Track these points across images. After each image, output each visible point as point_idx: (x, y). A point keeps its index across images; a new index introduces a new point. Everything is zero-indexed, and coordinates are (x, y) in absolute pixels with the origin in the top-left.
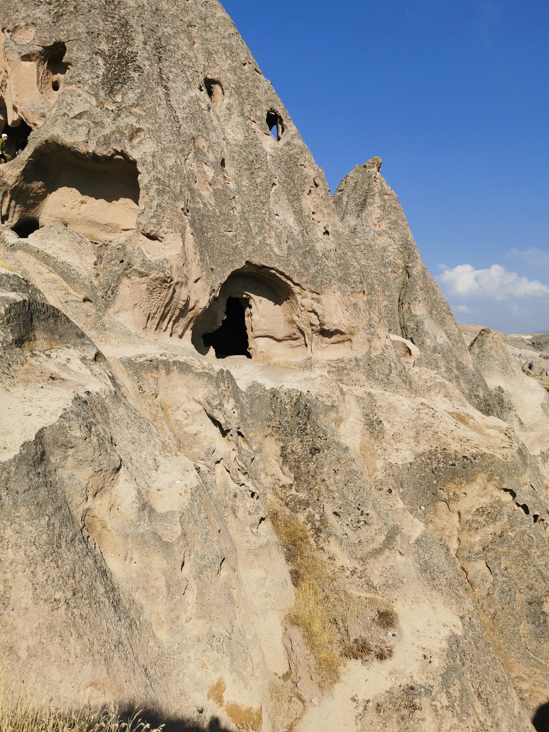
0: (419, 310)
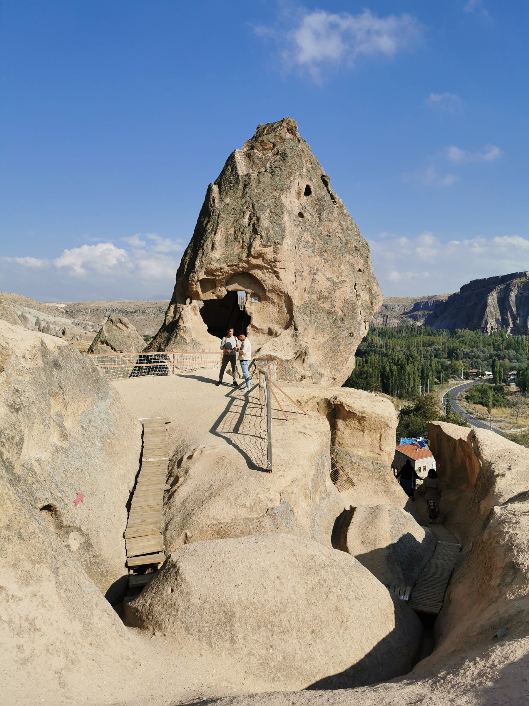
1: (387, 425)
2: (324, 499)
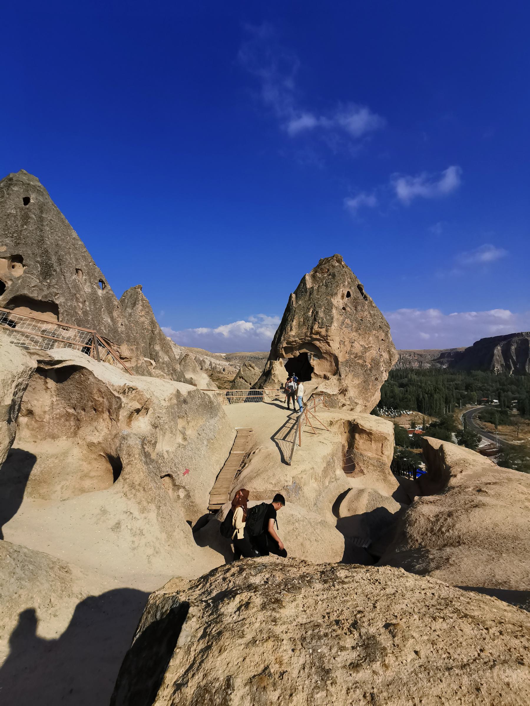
0: (157, 348)
1: (386, 438)
2: (333, 482)
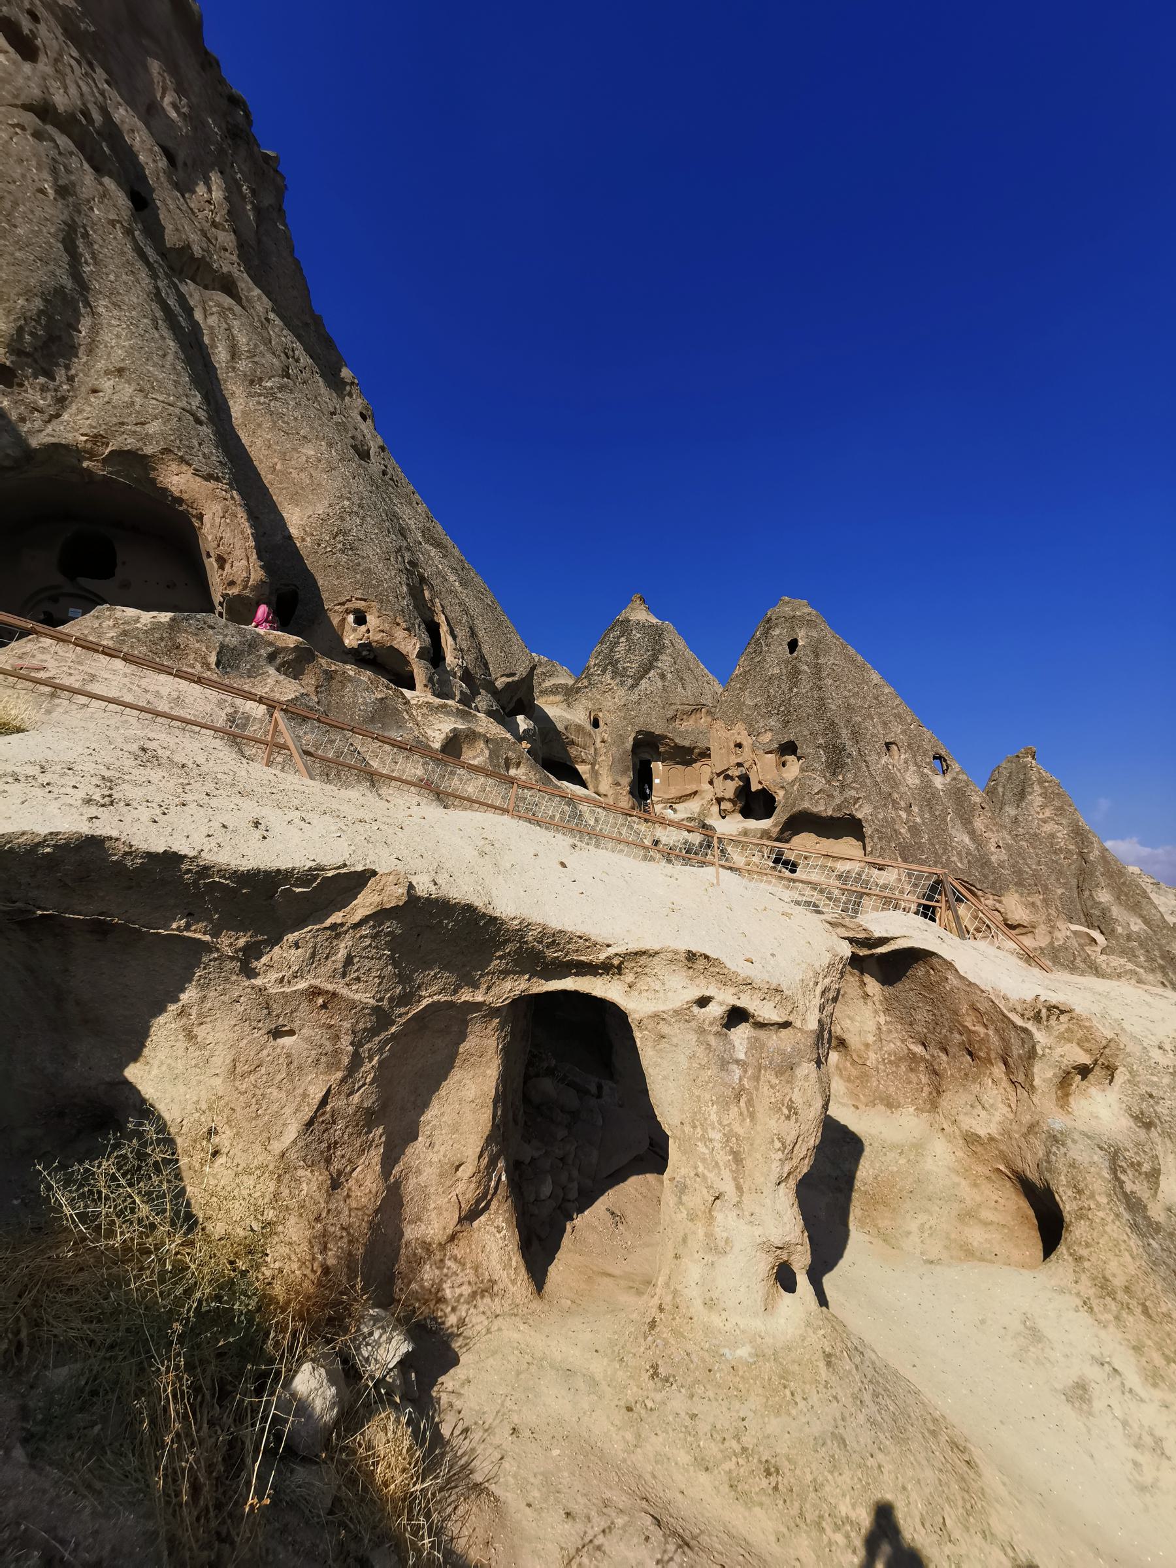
0: (1104, 896)
